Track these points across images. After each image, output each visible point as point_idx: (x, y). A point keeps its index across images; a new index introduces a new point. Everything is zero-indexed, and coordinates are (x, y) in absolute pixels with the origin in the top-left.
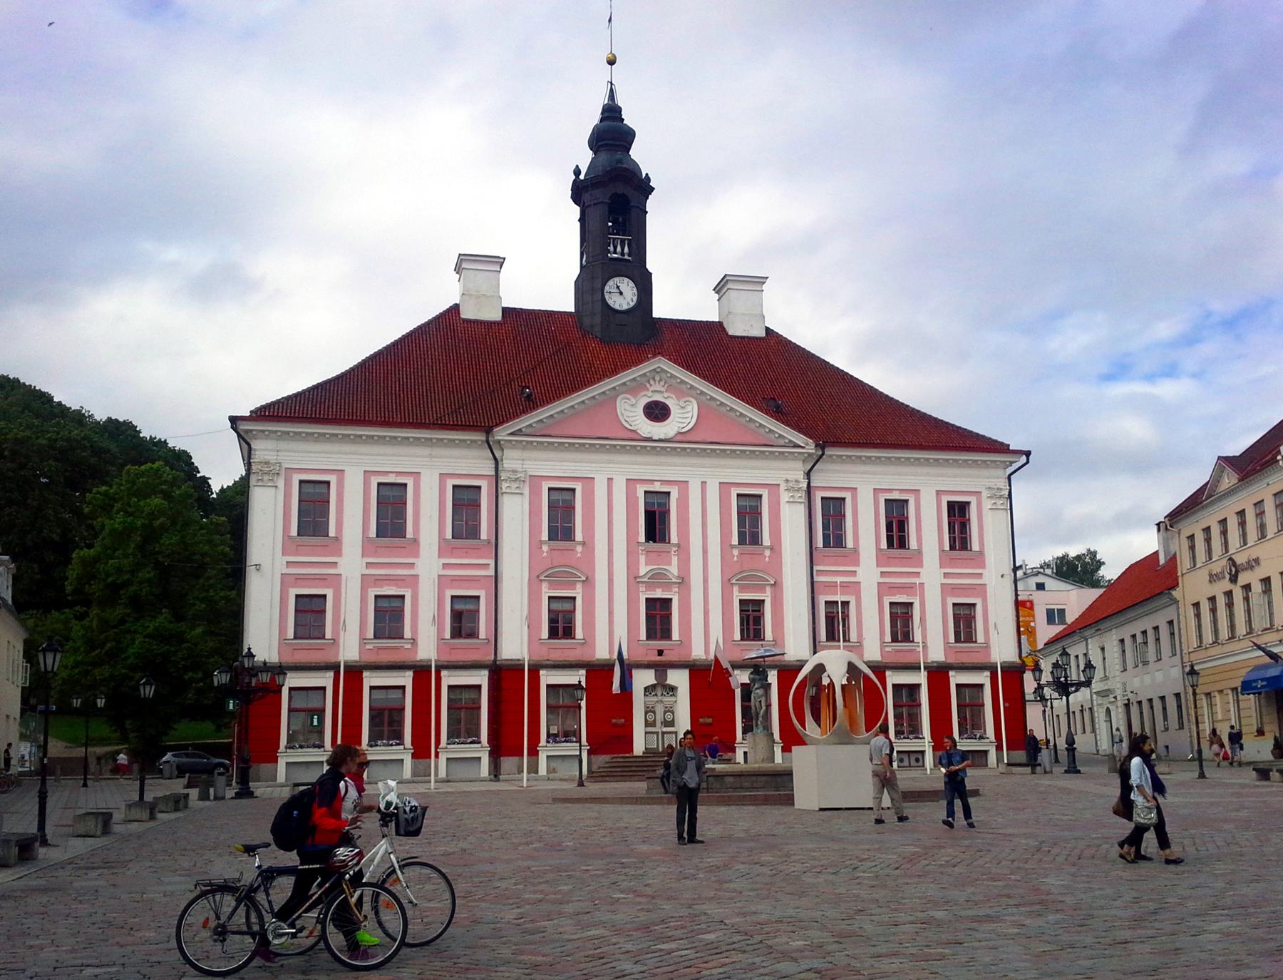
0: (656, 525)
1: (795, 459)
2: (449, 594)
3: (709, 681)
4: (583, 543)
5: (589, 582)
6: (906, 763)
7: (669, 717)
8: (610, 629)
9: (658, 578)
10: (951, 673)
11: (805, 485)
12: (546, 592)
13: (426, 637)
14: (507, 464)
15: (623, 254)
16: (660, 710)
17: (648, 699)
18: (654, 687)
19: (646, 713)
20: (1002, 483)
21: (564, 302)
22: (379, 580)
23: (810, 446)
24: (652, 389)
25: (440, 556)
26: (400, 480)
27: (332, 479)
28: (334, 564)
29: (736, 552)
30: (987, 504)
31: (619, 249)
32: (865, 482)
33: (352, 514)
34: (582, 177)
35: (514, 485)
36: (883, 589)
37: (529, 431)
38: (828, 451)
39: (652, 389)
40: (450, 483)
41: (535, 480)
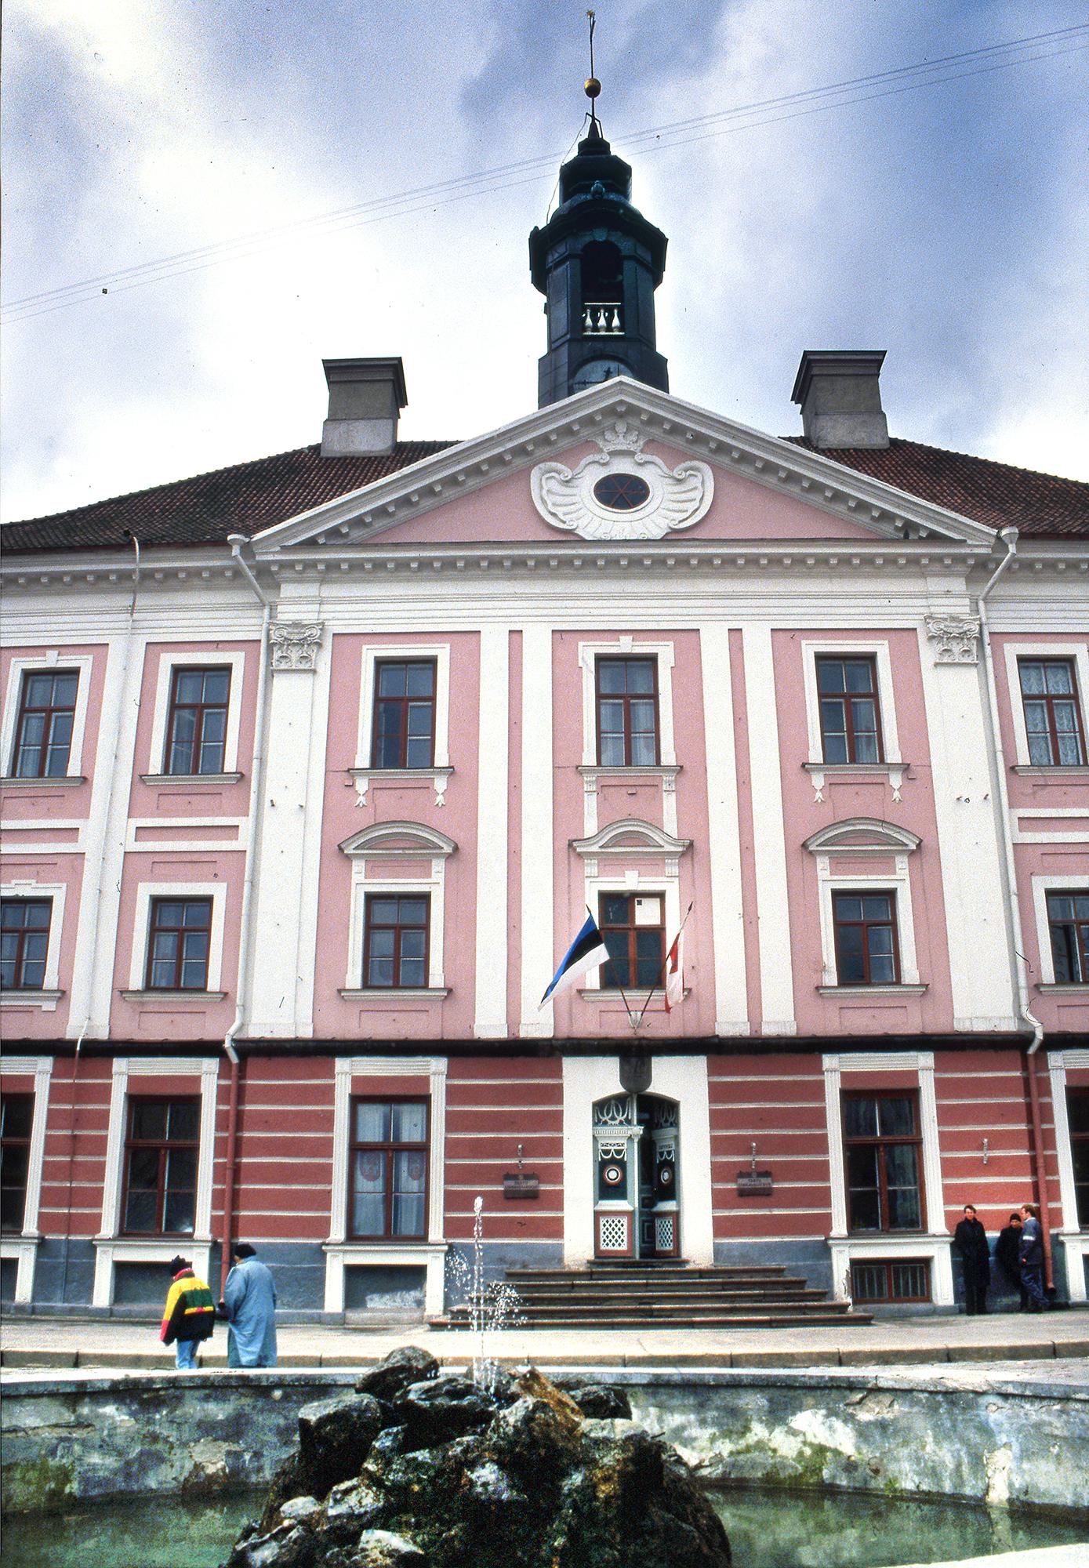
1: (947, 572)
4: (450, 771)
5: (459, 855)
8: (512, 968)
12: (361, 881)
15: (609, 328)
18: (619, 1101)
24: (611, 448)
26: (66, 662)
29: (818, 780)
31: (602, 322)
35: (295, 654)
40: (168, 660)
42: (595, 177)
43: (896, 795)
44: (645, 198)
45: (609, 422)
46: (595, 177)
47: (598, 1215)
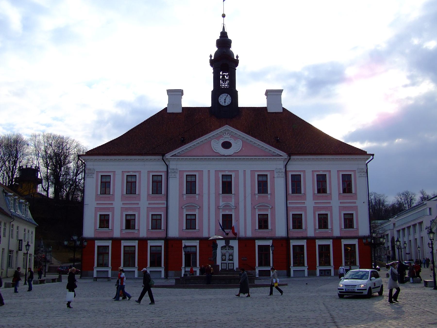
0: (227, 187)
2: (151, 213)
3: (246, 244)
6: (323, 274)
7: (231, 258)
9: (227, 206)
10: (342, 240)
11: (284, 170)
12: (185, 212)
13: (143, 229)
14: (171, 167)
16: (227, 255)
17: (222, 251)
18: (225, 246)
19: (222, 256)
20: (364, 166)
21: (207, 103)
22: (127, 209)
23: (285, 155)
24: (225, 137)
25: (147, 201)
27: (111, 174)
28: (112, 204)
29: (257, 196)
30: (358, 175)
32: (308, 168)
33: (118, 186)
34: (213, 58)
35: (173, 174)
36: (315, 209)
37: (179, 155)
38: (292, 157)
39: (225, 137)
40: (151, 174)
41: (181, 172)
42: (224, 42)
43: (269, 199)
44: (235, 49)
45: (225, 132)
46: (224, 42)
47: (221, 263)
